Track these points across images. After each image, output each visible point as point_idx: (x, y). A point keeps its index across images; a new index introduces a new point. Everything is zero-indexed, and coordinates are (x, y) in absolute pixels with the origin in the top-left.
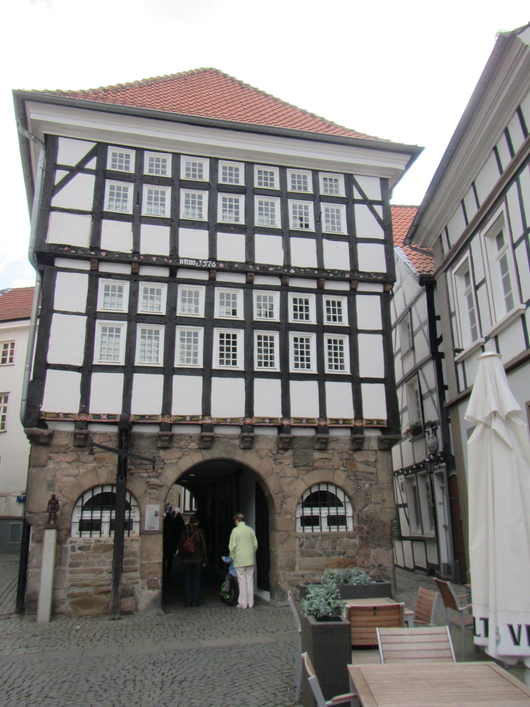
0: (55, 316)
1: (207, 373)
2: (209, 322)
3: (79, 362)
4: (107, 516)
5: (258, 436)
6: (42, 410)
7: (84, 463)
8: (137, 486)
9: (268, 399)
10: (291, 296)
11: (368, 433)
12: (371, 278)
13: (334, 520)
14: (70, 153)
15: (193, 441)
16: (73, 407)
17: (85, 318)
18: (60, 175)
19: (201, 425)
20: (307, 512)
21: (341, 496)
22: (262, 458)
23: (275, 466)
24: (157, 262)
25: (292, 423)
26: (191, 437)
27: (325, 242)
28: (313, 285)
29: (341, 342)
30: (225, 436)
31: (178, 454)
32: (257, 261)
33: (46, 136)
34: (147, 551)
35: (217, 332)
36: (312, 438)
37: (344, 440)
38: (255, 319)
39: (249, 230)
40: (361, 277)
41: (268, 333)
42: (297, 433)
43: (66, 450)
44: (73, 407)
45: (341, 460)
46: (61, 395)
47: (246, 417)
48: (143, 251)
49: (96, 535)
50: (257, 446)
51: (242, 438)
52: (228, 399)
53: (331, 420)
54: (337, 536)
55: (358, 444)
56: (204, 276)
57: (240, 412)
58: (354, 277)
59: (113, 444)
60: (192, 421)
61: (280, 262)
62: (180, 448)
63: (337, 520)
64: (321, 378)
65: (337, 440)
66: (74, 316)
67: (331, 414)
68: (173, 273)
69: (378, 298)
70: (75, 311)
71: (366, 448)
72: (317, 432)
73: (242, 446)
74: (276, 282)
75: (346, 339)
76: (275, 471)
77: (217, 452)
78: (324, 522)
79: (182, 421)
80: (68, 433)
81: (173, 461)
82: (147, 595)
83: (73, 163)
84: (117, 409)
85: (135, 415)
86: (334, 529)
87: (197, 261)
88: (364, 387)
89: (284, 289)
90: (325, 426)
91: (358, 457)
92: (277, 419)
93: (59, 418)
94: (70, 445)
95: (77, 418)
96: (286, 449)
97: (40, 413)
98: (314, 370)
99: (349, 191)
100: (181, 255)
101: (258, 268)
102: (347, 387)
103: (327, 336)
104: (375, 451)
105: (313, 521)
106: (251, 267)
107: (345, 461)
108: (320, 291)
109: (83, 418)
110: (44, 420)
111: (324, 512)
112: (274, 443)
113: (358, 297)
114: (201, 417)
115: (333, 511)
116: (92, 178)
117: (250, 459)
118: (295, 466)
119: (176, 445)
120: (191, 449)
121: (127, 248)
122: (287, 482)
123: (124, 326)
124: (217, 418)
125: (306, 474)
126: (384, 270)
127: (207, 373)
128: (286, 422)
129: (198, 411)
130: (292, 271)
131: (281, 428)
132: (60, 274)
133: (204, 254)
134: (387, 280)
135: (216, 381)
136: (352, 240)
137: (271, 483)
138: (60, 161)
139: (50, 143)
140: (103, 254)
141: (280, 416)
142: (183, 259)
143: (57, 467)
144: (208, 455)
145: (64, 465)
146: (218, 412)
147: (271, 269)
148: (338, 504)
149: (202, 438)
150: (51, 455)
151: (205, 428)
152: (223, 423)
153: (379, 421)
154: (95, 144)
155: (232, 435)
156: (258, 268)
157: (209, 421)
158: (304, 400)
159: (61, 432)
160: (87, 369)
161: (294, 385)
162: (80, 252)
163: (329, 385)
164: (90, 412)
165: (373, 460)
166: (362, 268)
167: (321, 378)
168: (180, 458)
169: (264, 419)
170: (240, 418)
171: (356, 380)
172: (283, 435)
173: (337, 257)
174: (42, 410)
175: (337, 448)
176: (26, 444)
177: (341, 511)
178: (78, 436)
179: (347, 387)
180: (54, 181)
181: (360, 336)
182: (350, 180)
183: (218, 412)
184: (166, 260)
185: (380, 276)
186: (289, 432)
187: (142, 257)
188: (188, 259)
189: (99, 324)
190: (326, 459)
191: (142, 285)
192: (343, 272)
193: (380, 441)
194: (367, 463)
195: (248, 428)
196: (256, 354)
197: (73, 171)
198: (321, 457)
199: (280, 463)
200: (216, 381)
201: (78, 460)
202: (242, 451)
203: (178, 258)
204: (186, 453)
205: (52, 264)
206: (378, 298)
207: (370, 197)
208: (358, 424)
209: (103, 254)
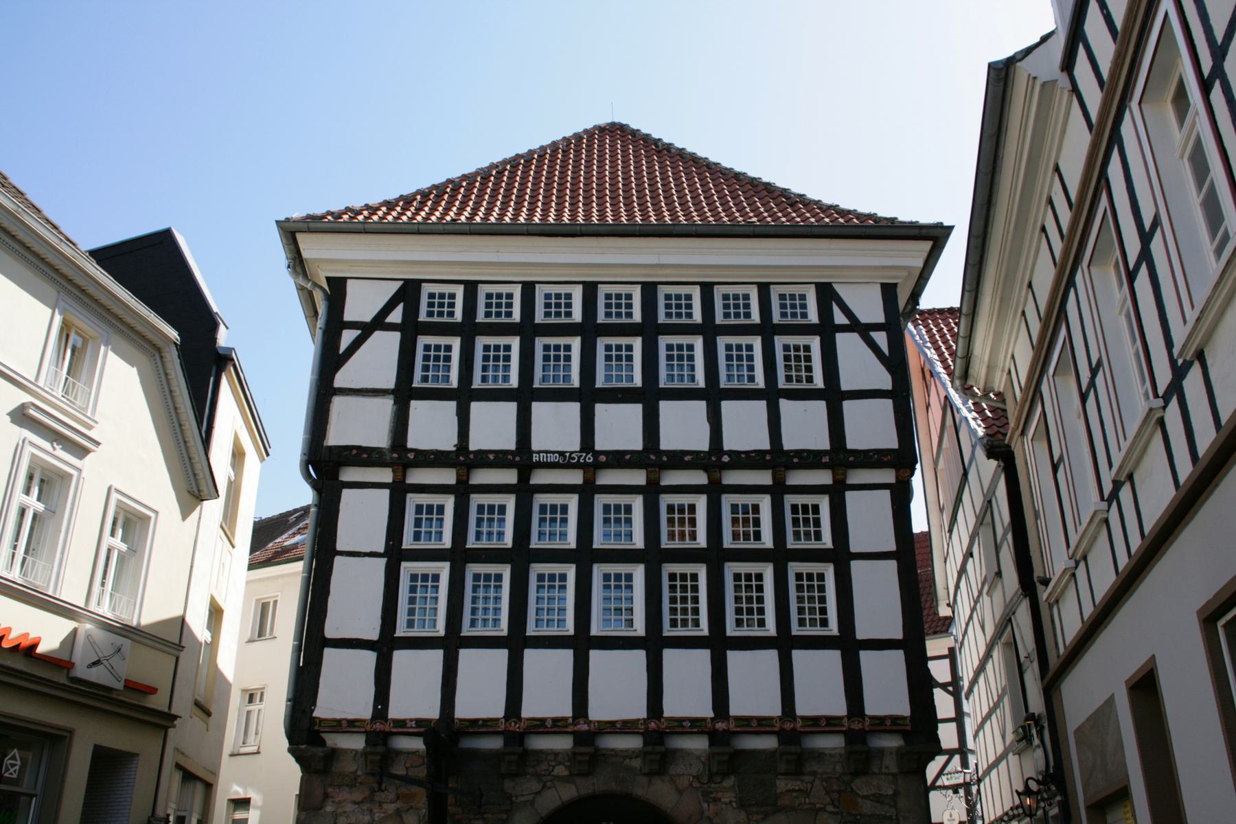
0: (338, 560)
3: (372, 631)
5: (675, 752)
6: (315, 714)
7: (380, 804)
10: (727, 500)
15: (560, 763)
16: (362, 708)
17: (383, 561)
18: (348, 337)
19: (573, 733)
22: (680, 792)
23: (705, 805)
24: (499, 459)
25: (732, 726)
26: (556, 754)
27: (784, 403)
28: (764, 478)
29: (821, 577)
30: (615, 753)
31: (535, 786)
32: (664, 446)
33: (328, 279)
36: (772, 753)
37: (831, 755)
38: (663, 546)
39: (649, 397)
40: (851, 459)
43: (353, 783)
44: (362, 708)
45: (827, 793)
46: (346, 688)
47: (649, 718)
48: (473, 446)
50: (677, 769)
53: (804, 718)
56: (576, 477)
58: (840, 457)
59: (422, 773)
60: (555, 726)
61: (703, 445)
62: (538, 776)
64: (785, 644)
65: (819, 755)
66: (367, 558)
67: (803, 708)
68: (524, 477)
69: (886, 494)
70: (368, 550)
71: (876, 770)
72: (781, 742)
73: (646, 771)
74: (700, 478)
75: (829, 571)
76: (706, 814)
77: (599, 783)
79: (541, 726)
80: (356, 751)
81: (526, 798)
83: (367, 317)
84: (432, 711)
85: (461, 720)
87: (562, 454)
88: (866, 657)
90: (794, 729)
91: (862, 786)
92: (704, 719)
93: (340, 726)
94: (359, 773)
95: (368, 728)
96: (725, 775)
97: (314, 720)
98: (771, 629)
99: (825, 312)
100: (535, 447)
101: (665, 459)
103: (794, 568)
104: (894, 775)
106: (653, 457)
107: (835, 795)
109: (378, 726)
110: (319, 732)
112: (704, 764)
113: (849, 495)
114: (570, 721)
116: (397, 336)
117: (661, 793)
118: (743, 805)
119: (531, 770)
120: (557, 777)
121: (447, 441)
123: (444, 569)
124: (599, 722)
125: (763, 819)
126: (894, 445)
128: (720, 726)
130: (726, 459)
131: (715, 737)
132: (346, 494)
133: (571, 442)
134: (902, 459)
135: (597, 657)
136: (834, 396)
138: (348, 316)
139: (337, 288)
140: (411, 456)
141: (711, 714)
142: (539, 452)
143: (340, 810)
144: (588, 786)
145: (349, 807)
146: (598, 711)
147: (687, 458)
149: (573, 756)
150: (330, 790)
153: (895, 719)
154: (400, 283)
155: (627, 751)
156: (665, 459)
157: (585, 727)
158: (754, 685)
159: (345, 751)
160: (385, 645)
161: (734, 658)
162: (375, 456)
163: (799, 657)
164: (390, 717)
165: (890, 792)
167: (785, 644)
168: (537, 793)
169: (680, 720)
170: (638, 720)
171: (849, 645)
172: (716, 749)
173: (805, 426)
174: (315, 714)
175: (821, 771)
176: (293, 772)
178: (370, 757)
180: (338, 348)
181: (855, 565)
182: (826, 294)
184: (510, 457)
185: (886, 456)
186: (728, 744)
187: (472, 456)
188: (547, 452)
189: (407, 568)
190: (800, 790)
191: (476, 499)
192: (818, 454)
194: (878, 798)
196: (666, 605)
197: (367, 330)
198: (790, 787)
199: (716, 800)
200: (597, 657)
201: (370, 799)
202: (643, 780)
203: (531, 452)
204: (549, 784)
205: (335, 476)
206: (886, 494)
207: (864, 319)
208: (856, 726)
209: (411, 456)
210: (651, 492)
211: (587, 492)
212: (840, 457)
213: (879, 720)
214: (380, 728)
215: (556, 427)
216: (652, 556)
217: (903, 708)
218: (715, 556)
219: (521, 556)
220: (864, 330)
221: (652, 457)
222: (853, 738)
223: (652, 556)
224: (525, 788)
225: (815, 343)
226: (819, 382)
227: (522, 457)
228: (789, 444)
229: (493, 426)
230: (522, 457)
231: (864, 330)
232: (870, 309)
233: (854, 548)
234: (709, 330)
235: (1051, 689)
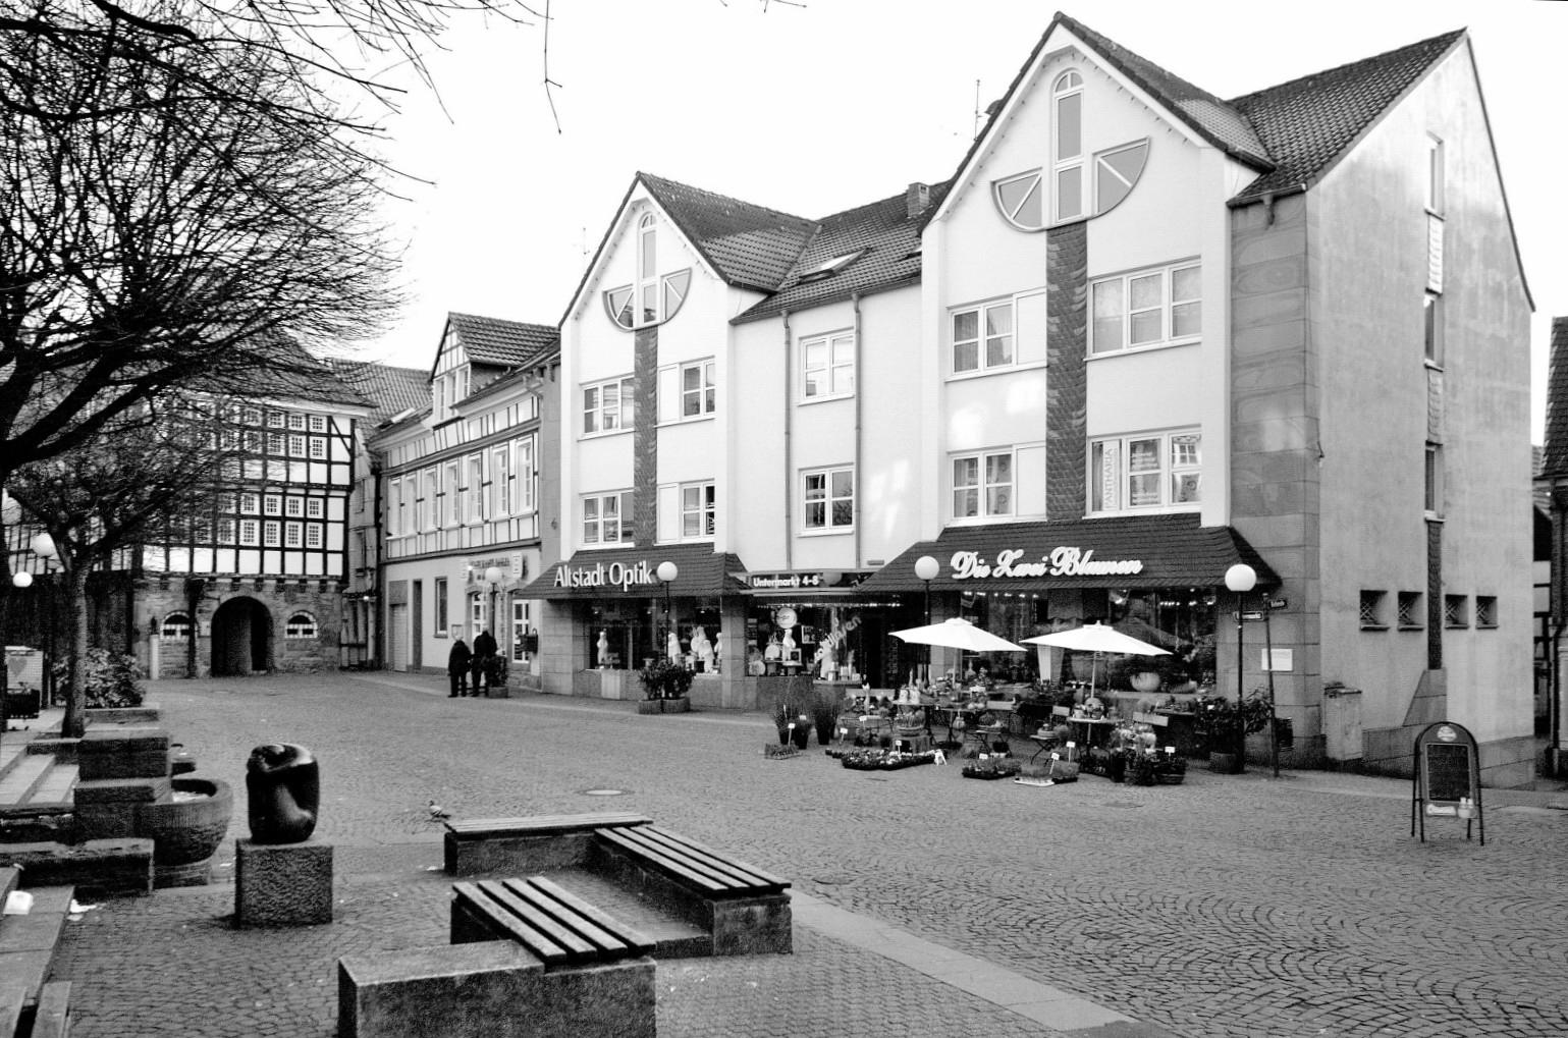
4: (179, 627)
11: (330, 583)
12: (338, 488)
20: (291, 627)
21: (311, 618)
27: (312, 464)
28: (302, 492)
34: (205, 647)
35: (242, 522)
41: (273, 522)
42: (288, 582)
49: (173, 638)
51: (256, 586)
52: (249, 563)
54: (309, 640)
55: (323, 588)
57: (256, 571)
58: (329, 486)
64: (305, 550)
65: (311, 586)
67: (309, 572)
78: (301, 633)
79: (223, 575)
82: (203, 668)
86: (306, 636)
89: (284, 494)
91: (324, 596)
98: (300, 545)
99: (329, 429)
102: (320, 556)
105: (294, 632)
108: (306, 496)
111: (301, 627)
115: (306, 627)
118: (286, 601)
122: (281, 610)
129: (233, 570)
137: (272, 610)
144: (236, 594)
146: (243, 571)
148: (308, 622)
152: (246, 576)
166: (333, 482)
171: (325, 552)
173: (318, 474)
177: (310, 627)
179: (320, 556)
182: (330, 420)
183: (243, 571)
193: (337, 588)
195: (259, 581)
201: (163, 597)
212: (329, 486)
213: (332, 576)
216: (262, 518)
218: (283, 519)
220: (341, 436)
222: (323, 582)
223: (262, 518)
225: (324, 440)
226: (324, 457)
228: (312, 481)
231: (341, 436)
232: (345, 429)
233: (329, 518)
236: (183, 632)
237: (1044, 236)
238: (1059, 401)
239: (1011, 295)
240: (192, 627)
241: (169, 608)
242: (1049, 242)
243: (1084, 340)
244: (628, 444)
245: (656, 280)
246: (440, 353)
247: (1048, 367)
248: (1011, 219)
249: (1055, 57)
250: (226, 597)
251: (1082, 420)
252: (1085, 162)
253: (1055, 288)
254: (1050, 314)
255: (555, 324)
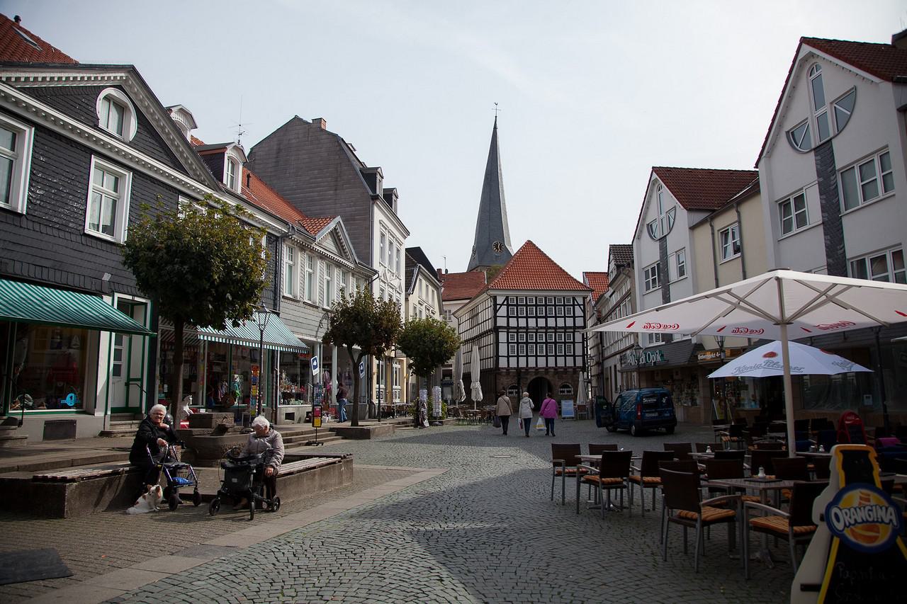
1: (536, 356)
2: (536, 343)
8: (522, 384)
9: (551, 362)
13: (568, 392)
14: (500, 301)
18: (498, 307)
39: (546, 317)
50: (550, 373)
52: (542, 362)
58: (575, 328)
63: (570, 392)
64: (565, 356)
77: (539, 376)
79: (531, 368)
91: (575, 376)
93: (502, 368)
105: (564, 392)
117: (548, 377)
127: (536, 356)
136: (574, 317)
137: (552, 383)
144: (537, 376)
148: (569, 387)
149: (535, 372)
151: (537, 370)
167: (565, 356)
171: (574, 356)
173: (570, 322)
182: (574, 299)
195: (547, 369)
197: (501, 305)
210: (546, 333)
211: (536, 333)
212: (575, 328)
214: (508, 369)
215: (532, 323)
216: (546, 343)
217: (581, 365)
218: (555, 343)
219: (527, 343)
220: (579, 305)
221: (547, 328)
223: (546, 343)
224: (528, 377)
227: (527, 328)
229: (522, 323)
230: (527, 328)
232: (580, 301)
234: (555, 305)
235: (603, 360)
236: (516, 392)
237: (813, 153)
238: (830, 241)
239: (802, 189)
240: (519, 390)
241: (510, 382)
242: (816, 156)
243: (839, 205)
244: (660, 292)
245: (664, 215)
246: (609, 263)
247: (823, 223)
248: (798, 148)
249: (805, 59)
250: (532, 378)
251: (843, 250)
252: (826, 108)
253: (821, 179)
254: (821, 194)
255: (631, 244)
